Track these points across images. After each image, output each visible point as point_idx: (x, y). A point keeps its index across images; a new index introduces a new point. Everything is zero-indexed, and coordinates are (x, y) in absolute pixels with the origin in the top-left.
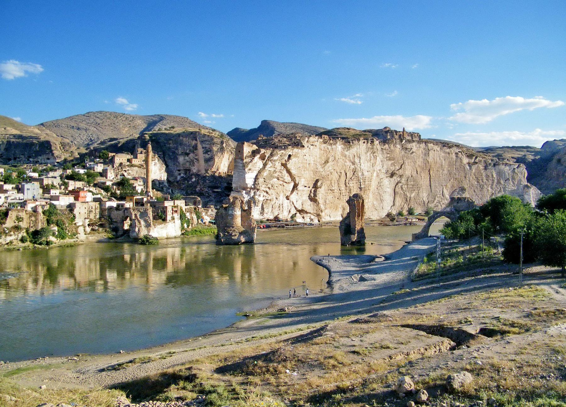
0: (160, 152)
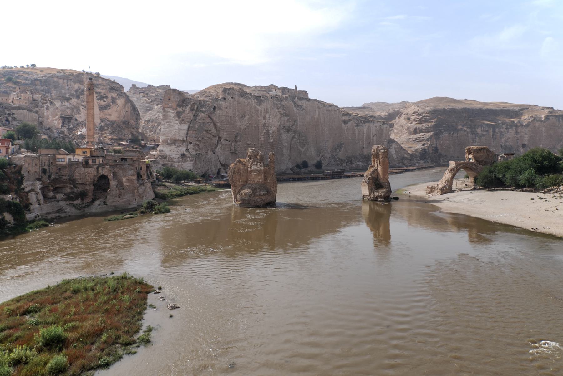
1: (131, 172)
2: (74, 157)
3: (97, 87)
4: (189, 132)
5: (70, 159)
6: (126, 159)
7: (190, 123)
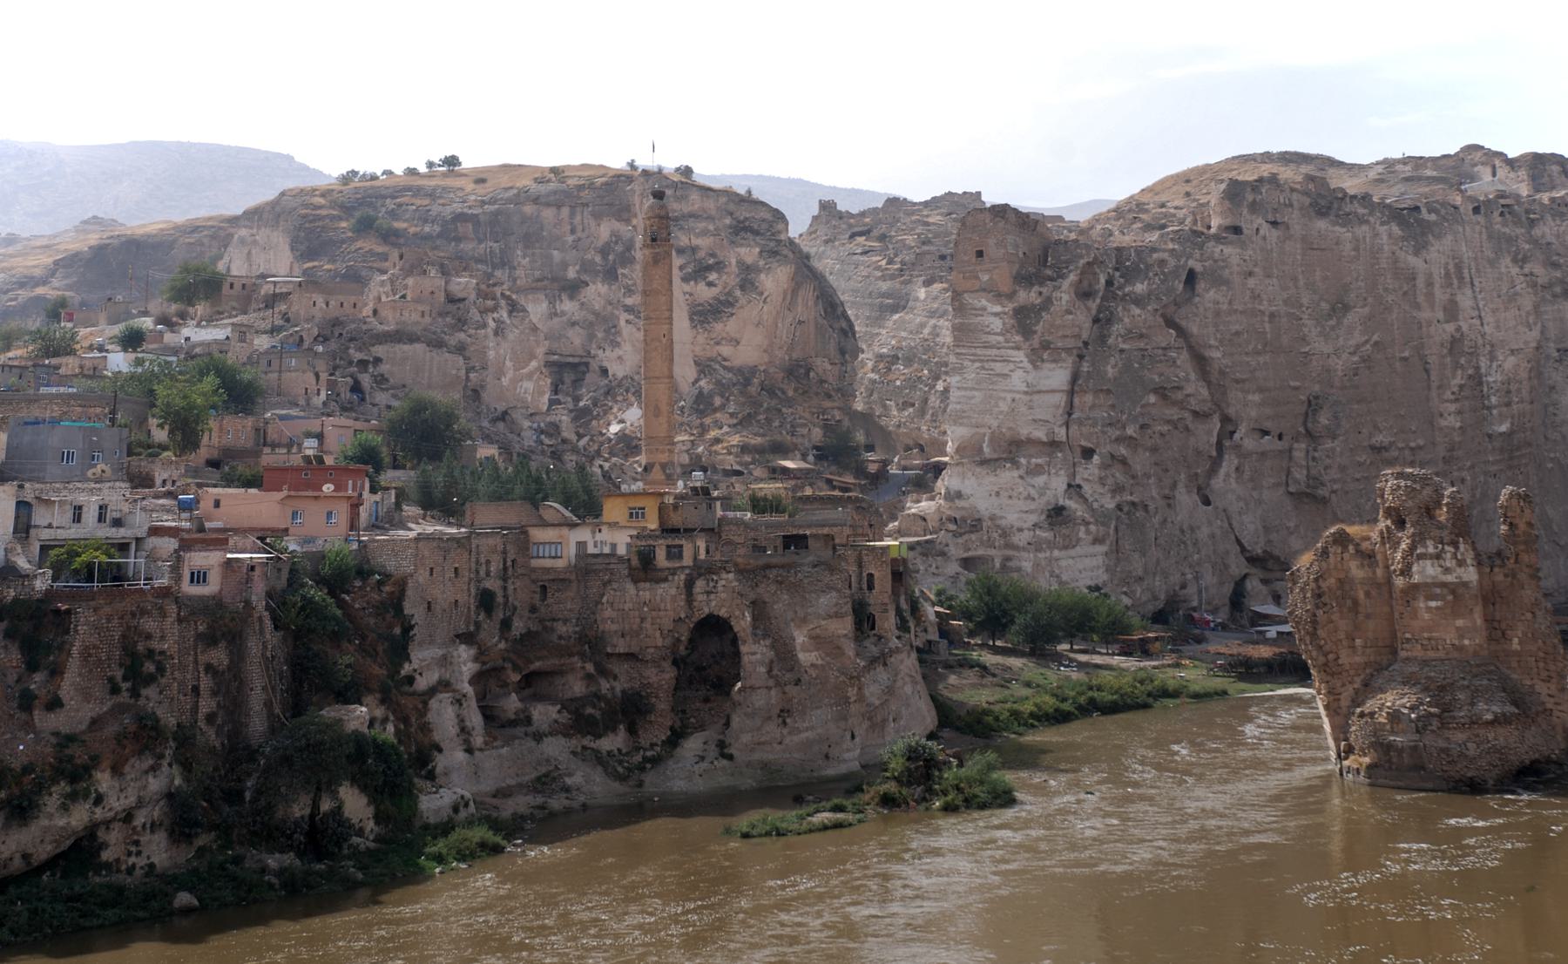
1: (826, 601)
2: (598, 537)
3: (682, 228)
4: (1076, 400)
5: (581, 545)
6: (805, 537)
7: (1081, 357)
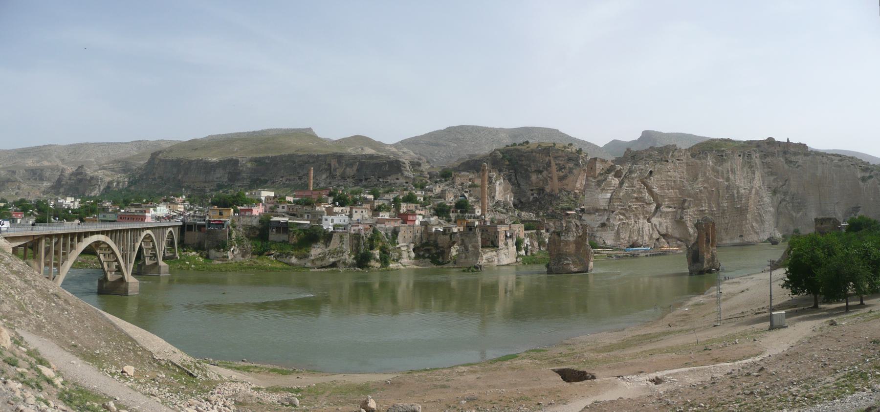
0: (512, 169)
4: (611, 201)
